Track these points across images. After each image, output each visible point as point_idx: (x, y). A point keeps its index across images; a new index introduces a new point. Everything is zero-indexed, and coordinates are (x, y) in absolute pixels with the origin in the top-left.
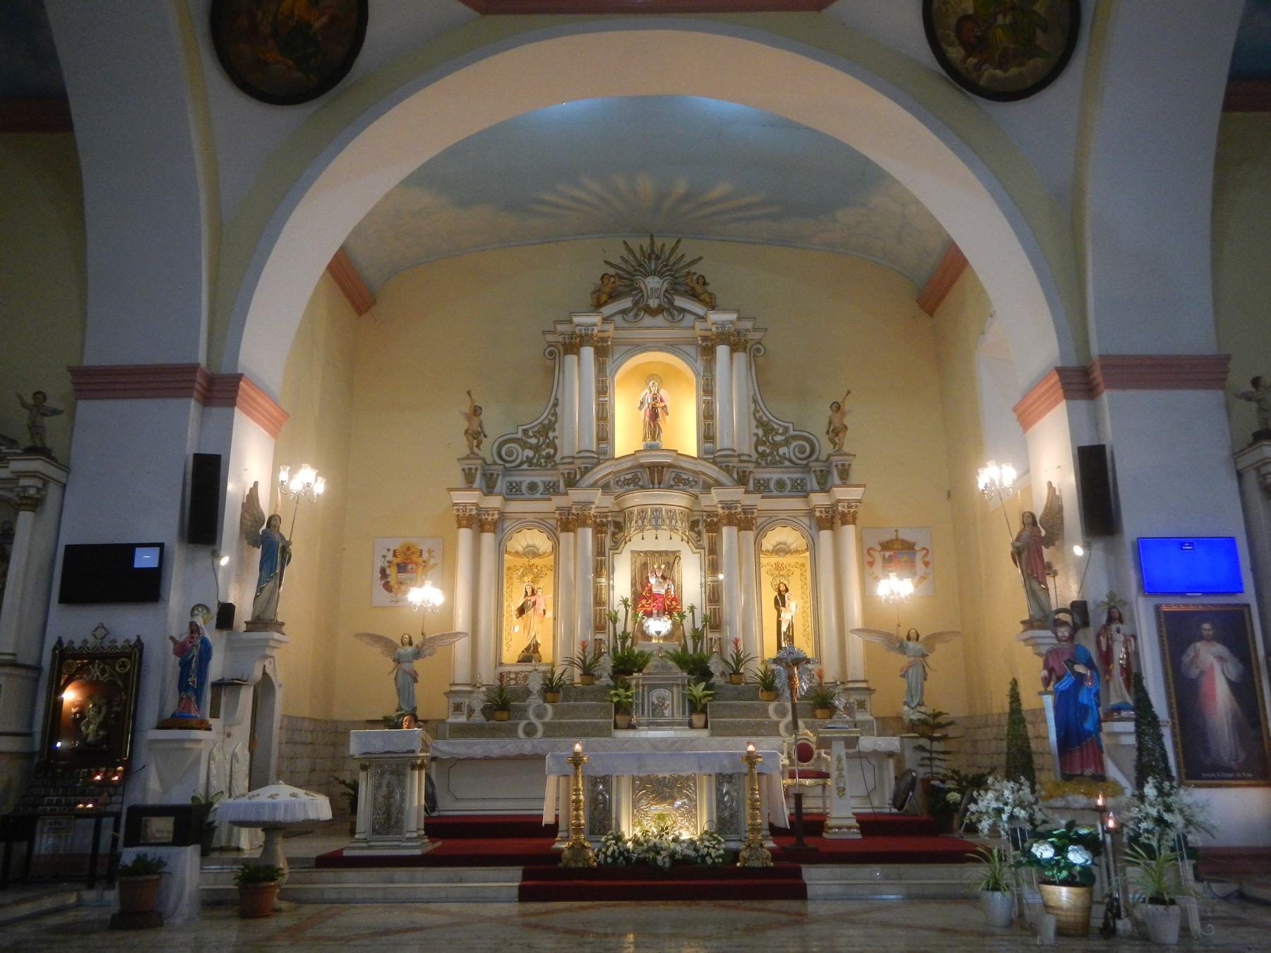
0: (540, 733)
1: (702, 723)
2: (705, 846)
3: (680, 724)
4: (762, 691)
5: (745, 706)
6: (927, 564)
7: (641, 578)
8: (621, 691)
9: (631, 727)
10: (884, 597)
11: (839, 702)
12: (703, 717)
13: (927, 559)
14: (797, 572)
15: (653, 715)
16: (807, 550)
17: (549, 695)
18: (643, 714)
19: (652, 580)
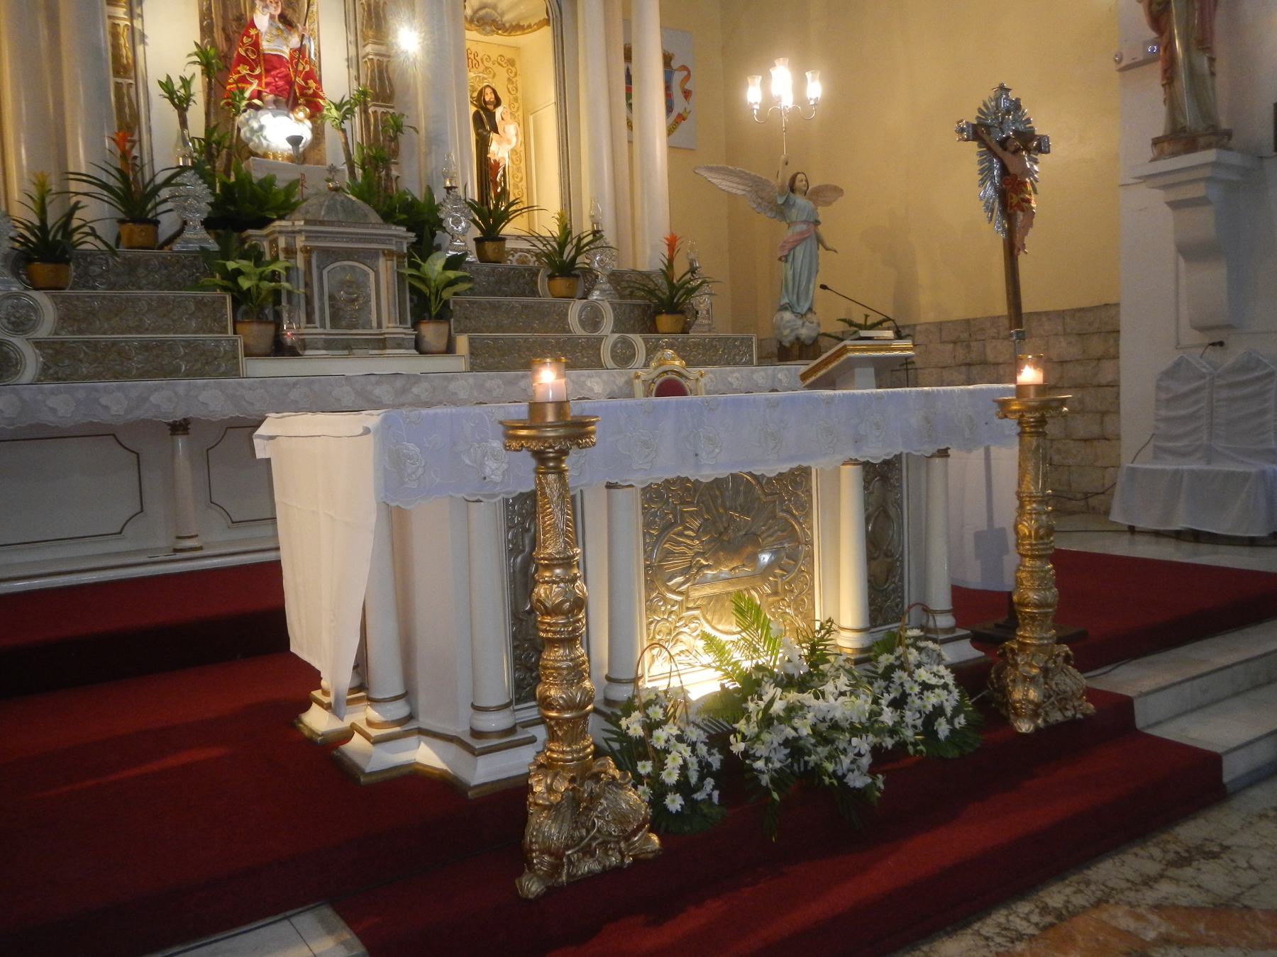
0: (30, 369)
1: (442, 344)
2: (926, 687)
3: (399, 345)
4: (551, 277)
5: (525, 307)
6: (687, 94)
7: (225, 18)
8: (245, 265)
9: (280, 349)
10: (757, 107)
11: (702, 302)
12: (443, 328)
13: (688, 87)
14: (502, 73)
15: (336, 319)
16: (547, 22)
17: (42, 270)
18: (310, 319)
19: (262, 20)
